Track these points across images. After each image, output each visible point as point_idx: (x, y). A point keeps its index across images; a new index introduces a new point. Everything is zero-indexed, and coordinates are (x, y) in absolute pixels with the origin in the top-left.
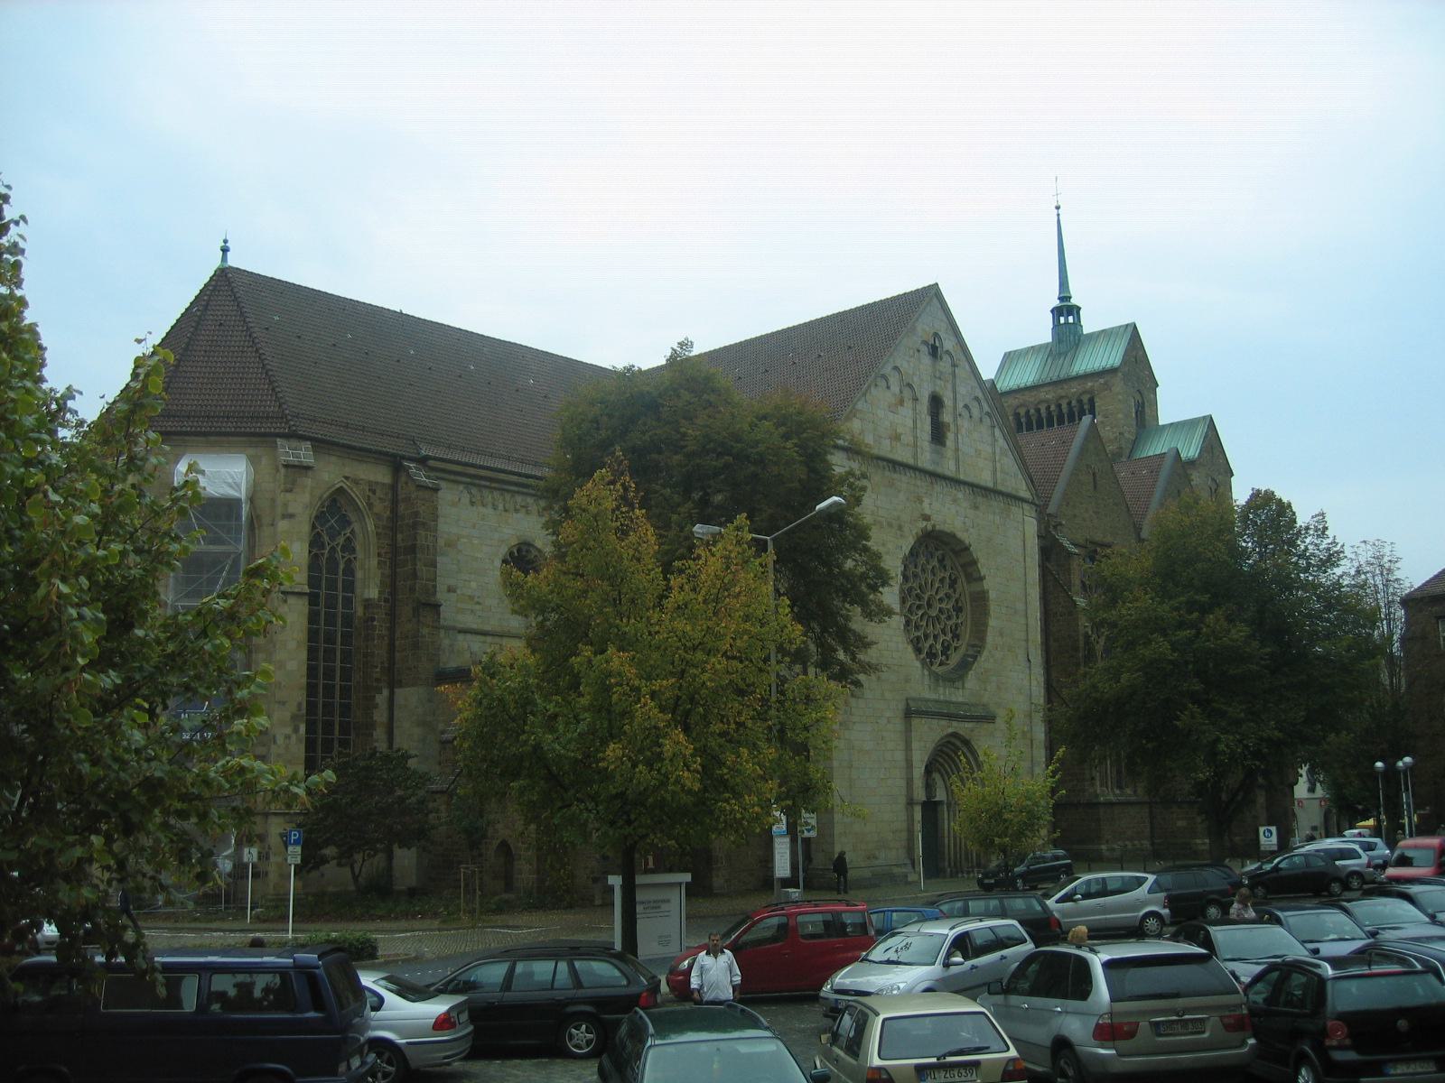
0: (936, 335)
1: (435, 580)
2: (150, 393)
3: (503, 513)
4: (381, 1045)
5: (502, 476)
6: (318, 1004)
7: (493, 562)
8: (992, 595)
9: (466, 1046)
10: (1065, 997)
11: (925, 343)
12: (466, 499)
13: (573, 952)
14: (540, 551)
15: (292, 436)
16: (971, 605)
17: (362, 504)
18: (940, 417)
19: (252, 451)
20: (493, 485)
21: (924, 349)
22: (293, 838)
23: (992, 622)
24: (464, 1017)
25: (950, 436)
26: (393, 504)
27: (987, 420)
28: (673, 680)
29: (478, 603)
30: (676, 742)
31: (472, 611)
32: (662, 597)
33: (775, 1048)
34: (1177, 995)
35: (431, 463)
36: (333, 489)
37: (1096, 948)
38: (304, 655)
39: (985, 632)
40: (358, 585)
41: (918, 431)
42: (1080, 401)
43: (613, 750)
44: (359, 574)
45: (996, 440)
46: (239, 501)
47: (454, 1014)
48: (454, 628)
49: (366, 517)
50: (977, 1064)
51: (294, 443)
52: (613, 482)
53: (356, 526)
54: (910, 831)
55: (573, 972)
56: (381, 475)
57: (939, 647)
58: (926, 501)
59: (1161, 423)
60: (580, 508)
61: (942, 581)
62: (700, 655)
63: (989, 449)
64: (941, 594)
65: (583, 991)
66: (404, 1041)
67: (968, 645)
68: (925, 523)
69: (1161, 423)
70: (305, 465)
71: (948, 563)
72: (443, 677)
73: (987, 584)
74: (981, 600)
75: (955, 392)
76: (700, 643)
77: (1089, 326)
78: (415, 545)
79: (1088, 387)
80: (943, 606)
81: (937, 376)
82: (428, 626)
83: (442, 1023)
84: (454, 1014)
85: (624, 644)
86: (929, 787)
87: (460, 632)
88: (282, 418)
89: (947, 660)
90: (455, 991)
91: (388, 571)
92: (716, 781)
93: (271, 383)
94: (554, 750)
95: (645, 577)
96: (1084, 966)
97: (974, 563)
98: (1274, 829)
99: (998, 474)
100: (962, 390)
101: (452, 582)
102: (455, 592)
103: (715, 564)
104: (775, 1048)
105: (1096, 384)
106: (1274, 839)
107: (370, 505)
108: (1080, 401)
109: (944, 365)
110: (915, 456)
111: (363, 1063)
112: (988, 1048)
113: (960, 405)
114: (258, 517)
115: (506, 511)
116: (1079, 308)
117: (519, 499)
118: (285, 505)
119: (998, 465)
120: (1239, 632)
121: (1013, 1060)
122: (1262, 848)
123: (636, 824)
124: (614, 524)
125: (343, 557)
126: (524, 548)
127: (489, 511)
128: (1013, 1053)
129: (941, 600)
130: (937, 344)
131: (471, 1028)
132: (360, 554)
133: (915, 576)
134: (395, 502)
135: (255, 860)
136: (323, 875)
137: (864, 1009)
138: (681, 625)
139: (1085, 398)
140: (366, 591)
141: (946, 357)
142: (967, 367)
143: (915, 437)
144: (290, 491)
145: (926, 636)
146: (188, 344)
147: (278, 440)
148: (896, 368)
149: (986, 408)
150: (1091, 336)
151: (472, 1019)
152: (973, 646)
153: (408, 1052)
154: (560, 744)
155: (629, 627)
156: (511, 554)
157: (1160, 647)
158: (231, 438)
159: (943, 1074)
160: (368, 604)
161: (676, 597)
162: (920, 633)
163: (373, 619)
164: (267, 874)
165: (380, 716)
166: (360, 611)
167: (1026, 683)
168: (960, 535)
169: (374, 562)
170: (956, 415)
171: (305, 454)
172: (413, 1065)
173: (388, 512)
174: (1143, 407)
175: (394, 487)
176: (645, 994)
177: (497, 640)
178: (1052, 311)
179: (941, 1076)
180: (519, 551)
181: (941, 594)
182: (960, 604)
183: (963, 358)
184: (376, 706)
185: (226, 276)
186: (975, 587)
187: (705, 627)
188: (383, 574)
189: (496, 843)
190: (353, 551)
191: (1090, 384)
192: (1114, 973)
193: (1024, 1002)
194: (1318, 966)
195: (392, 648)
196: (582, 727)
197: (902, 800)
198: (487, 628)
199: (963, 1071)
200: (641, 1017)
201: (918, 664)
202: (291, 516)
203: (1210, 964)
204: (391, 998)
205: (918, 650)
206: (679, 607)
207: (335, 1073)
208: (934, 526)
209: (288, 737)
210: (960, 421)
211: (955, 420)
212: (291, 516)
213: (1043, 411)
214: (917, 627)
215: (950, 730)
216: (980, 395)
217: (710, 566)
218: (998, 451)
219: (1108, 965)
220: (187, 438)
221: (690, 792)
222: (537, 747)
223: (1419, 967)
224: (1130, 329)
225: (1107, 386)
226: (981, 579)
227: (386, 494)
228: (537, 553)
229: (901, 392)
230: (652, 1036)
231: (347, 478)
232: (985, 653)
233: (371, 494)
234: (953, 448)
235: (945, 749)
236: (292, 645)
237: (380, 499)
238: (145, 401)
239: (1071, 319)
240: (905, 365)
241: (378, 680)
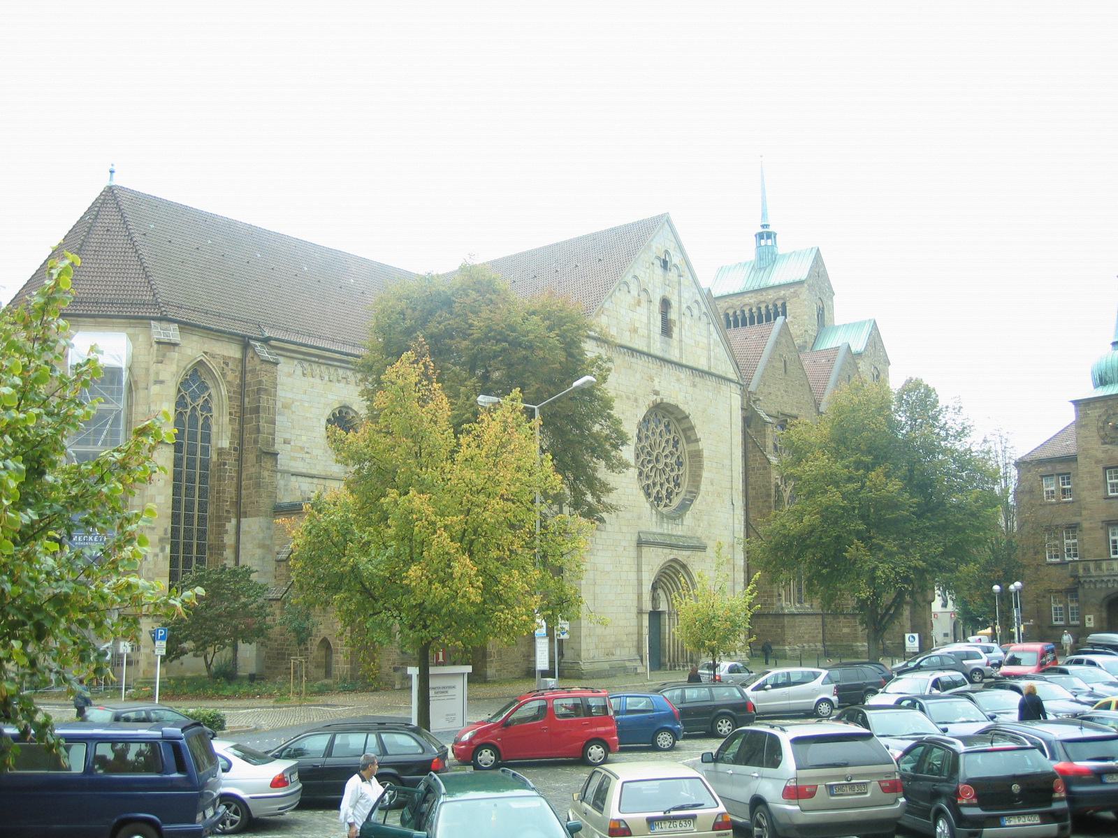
0: (666, 252)
1: (273, 434)
2: (61, 289)
3: (329, 383)
4: (228, 799)
5: (328, 354)
6: (181, 767)
8: (706, 453)
9: (295, 800)
10: (760, 764)
11: (658, 258)
12: (299, 371)
13: (382, 727)
14: (356, 413)
15: (163, 319)
16: (690, 462)
17: (217, 373)
18: (668, 315)
19: (131, 330)
20: (321, 361)
21: (658, 263)
22: (160, 635)
23: (705, 474)
24: (295, 777)
25: (676, 330)
27: (704, 318)
28: (462, 517)
29: (307, 453)
30: (463, 565)
32: (453, 452)
33: (539, 805)
34: (846, 765)
35: (273, 343)
36: (196, 361)
37: (785, 728)
38: (170, 491)
39: (699, 482)
40: (213, 437)
41: (652, 326)
42: (775, 306)
43: (414, 571)
44: (214, 429)
45: (710, 334)
46: (120, 369)
47: (287, 775)
48: (287, 472)
50: (694, 817)
51: (165, 325)
52: (416, 362)
53: (213, 391)
54: (640, 634)
55: (381, 743)
56: (233, 351)
57: (664, 492)
58: (657, 380)
59: (836, 324)
60: (392, 383)
61: (667, 441)
62: (482, 498)
63: (705, 341)
64: (667, 452)
65: (387, 757)
66: (248, 796)
67: (686, 491)
68: (655, 397)
69: (836, 324)
70: (173, 342)
71: (672, 427)
72: (281, 510)
73: (701, 445)
74: (697, 457)
75: (680, 296)
76: (482, 488)
77: (783, 245)
79: (782, 295)
80: (668, 461)
81: (666, 284)
83: (278, 782)
84: (287, 775)
85: (424, 488)
86: (654, 599)
87: (293, 475)
88: (156, 305)
89: (670, 502)
90: (289, 757)
91: (236, 426)
92: (493, 595)
93: (147, 277)
94: (368, 569)
95: (441, 436)
96: (775, 744)
97: (692, 428)
98: (916, 635)
99: (712, 360)
100: (686, 295)
101: (287, 436)
102: (289, 444)
103: (496, 427)
104: (539, 805)
105: (789, 292)
106: (916, 643)
107: (224, 375)
108: (775, 306)
109: (673, 275)
110: (649, 346)
111: (216, 813)
112: (703, 805)
113: (684, 306)
114: (136, 382)
116: (775, 234)
117: (341, 372)
118: (157, 374)
119: (712, 354)
120: (894, 486)
121: (722, 814)
122: (907, 650)
123: (431, 628)
124: (416, 394)
125: (202, 415)
126: (344, 410)
127: (318, 380)
128: (722, 809)
129: (666, 456)
130: (667, 259)
131: (300, 785)
132: (215, 413)
133: (647, 437)
134: (243, 373)
135: (129, 650)
136: (182, 664)
137: (607, 773)
138: (469, 474)
139: (779, 303)
140: (220, 441)
141: (673, 269)
142: (690, 278)
143: (649, 330)
144: (161, 362)
145: (654, 484)
146: (82, 245)
147: (152, 322)
148: (635, 277)
149: (704, 309)
150: (784, 256)
151: (301, 778)
152: (691, 492)
153: (251, 804)
154: (372, 565)
155: (428, 475)
156: (334, 415)
157: (834, 497)
158: (114, 320)
159: (668, 824)
160: (221, 452)
161: (464, 453)
162: (650, 482)
163: (225, 464)
164: (138, 662)
165: (229, 539)
166: (214, 457)
167: (731, 521)
168: (681, 406)
169: (226, 419)
170: (681, 314)
171: (173, 333)
172: (254, 815)
174: (823, 311)
175: (243, 361)
176: (436, 760)
177: (322, 481)
178: (756, 236)
179: (666, 826)
181: (667, 452)
182: (681, 460)
183: (686, 269)
184: (226, 532)
185: (113, 192)
186: (692, 447)
187: (487, 476)
188: (233, 429)
189: (318, 640)
190: (210, 410)
191: (783, 292)
192: (799, 747)
193: (730, 769)
194: (953, 743)
195: (239, 488)
196: (390, 552)
197: (634, 610)
198: (314, 472)
199: (683, 823)
200: (435, 779)
201: (648, 505)
202: (162, 382)
203: (872, 740)
204: (238, 763)
205: (648, 495)
206: (466, 460)
207: (194, 822)
208: (662, 399)
209: (157, 555)
210: (683, 319)
211: (680, 318)
212: (162, 382)
213: (747, 312)
214: (648, 477)
215: (672, 557)
216: (699, 299)
217: (491, 428)
218: (712, 342)
219: (796, 741)
220: (79, 319)
221: (473, 604)
222: (355, 568)
223: (1029, 745)
224: (814, 251)
225: (796, 295)
226: (697, 441)
227: (237, 366)
229: (639, 295)
230: (444, 794)
231: (206, 353)
232: (699, 497)
233: (224, 366)
234: (678, 339)
235: (667, 571)
236: (161, 483)
237: (232, 370)
238: (57, 295)
239: (769, 241)
240: (642, 274)
241: (228, 512)
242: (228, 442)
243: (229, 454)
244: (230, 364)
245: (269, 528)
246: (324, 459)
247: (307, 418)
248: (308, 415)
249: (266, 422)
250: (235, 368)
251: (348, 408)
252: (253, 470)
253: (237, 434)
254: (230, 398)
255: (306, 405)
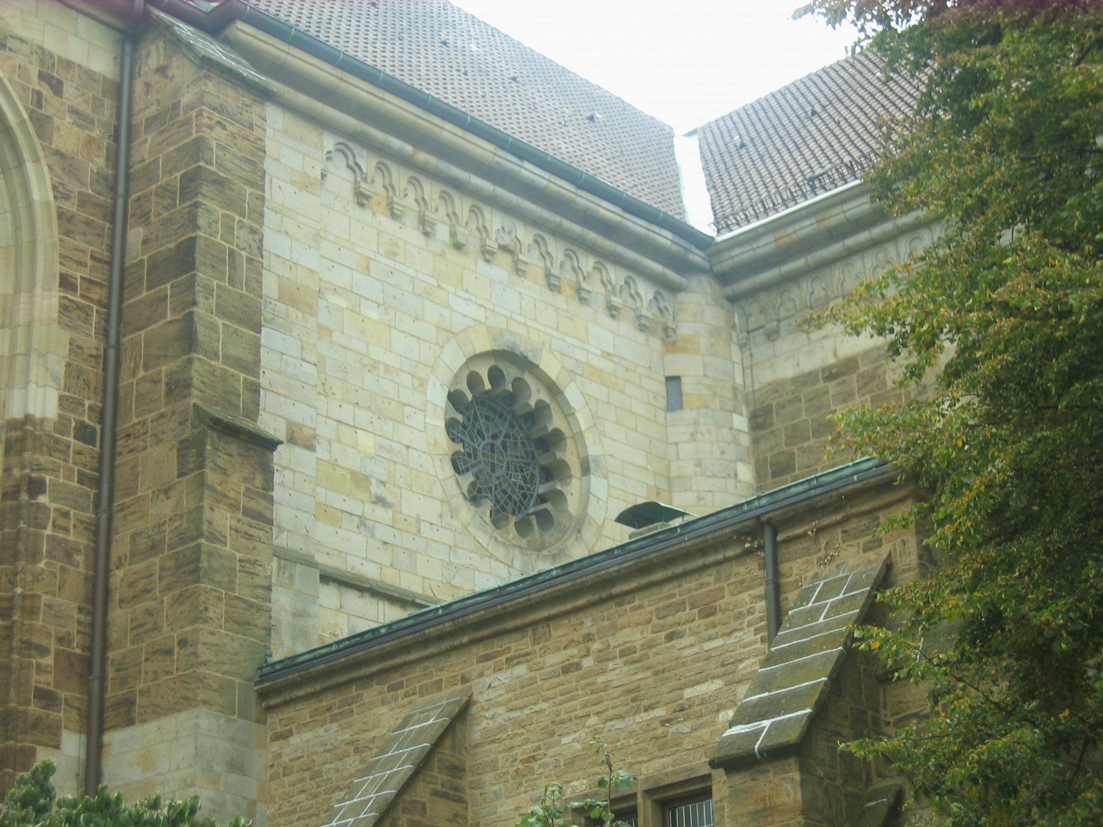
3: (452, 254)
5: (449, 133)
7: (423, 383)
12: (341, 180)
14: (554, 389)
20: (422, 157)
26: (116, 138)
29: (380, 501)
31: (363, 522)
49: (26, 155)
78: (193, 241)
82: (234, 507)
87: (326, 578)
101: (300, 414)
102: (310, 447)
107: (42, 124)
115: (458, 247)
117: (494, 221)
126: (510, 372)
127: (408, 233)
163: (36, 487)
169: (48, 300)
173: (101, 162)
180: (495, 375)
188: (75, 348)
227: (97, 106)
228: (544, 396)
233: (45, 90)
241: (47, 698)
242: (53, 397)
243: (56, 447)
244: (69, 90)
245: (237, 766)
246: (446, 536)
247: (375, 365)
248: (377, 354)
249: (222, 311)
250: (86, 108)
251: (526, 364)
252: (166, 508)
253: (92, 372)
254: (64, 218)
255: (373, 314)
